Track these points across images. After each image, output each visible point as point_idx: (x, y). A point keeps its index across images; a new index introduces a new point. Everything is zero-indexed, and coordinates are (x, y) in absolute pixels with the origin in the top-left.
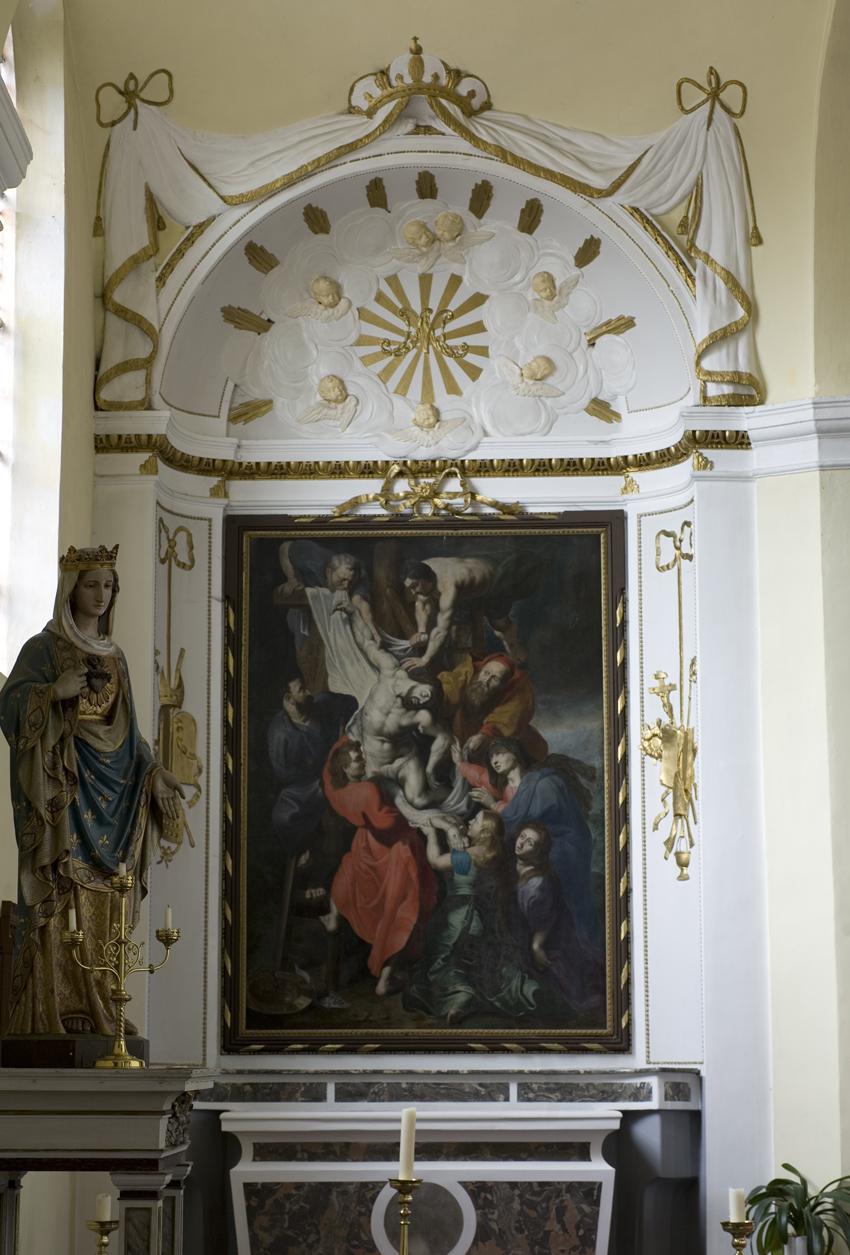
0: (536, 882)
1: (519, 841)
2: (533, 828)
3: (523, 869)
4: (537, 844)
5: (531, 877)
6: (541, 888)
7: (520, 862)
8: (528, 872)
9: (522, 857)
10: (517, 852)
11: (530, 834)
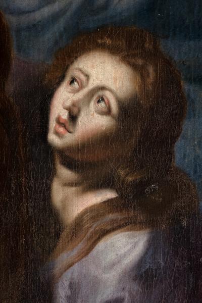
0: (125, 248)
1: (62, 100)
2: (113, 50)
3: (74, 201)
4: (128, 111)
5: (104, 233)
6: (143, 273)
7: (64, 173)
8: (95, 212)
9: (70, 158)
10: (52, 138)
11: (105, 74)
